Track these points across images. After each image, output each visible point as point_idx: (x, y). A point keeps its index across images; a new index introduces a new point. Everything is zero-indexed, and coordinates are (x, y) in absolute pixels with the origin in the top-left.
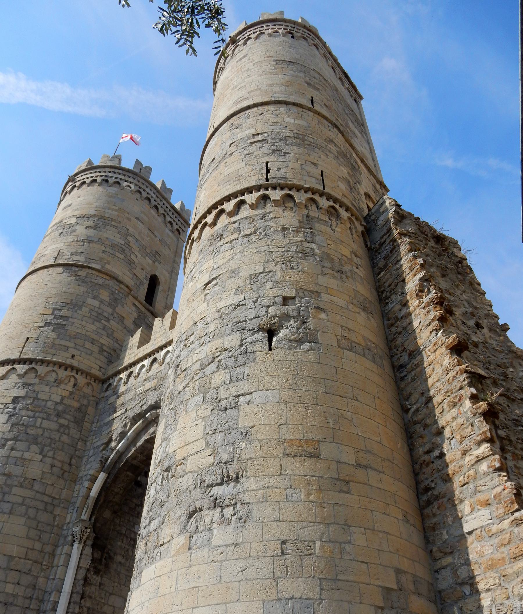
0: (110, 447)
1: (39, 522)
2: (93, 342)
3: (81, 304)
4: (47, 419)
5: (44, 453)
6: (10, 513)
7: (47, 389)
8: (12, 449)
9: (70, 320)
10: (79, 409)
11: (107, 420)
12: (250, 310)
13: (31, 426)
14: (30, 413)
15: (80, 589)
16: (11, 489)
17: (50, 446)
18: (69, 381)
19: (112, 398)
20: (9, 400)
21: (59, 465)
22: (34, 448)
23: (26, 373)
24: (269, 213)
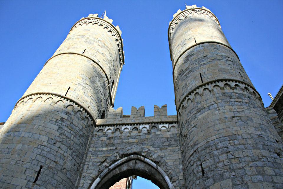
3: (94, 81)
4: (76, 137)
5: (73, 156)
7: (77, 120)
11: (101, 149)
12: (268, 142)
13: (69, 138)
18: (86, 120)
19: (103, 137)
21: (77, 165)
22: (69, 152)
24: (251, 97)
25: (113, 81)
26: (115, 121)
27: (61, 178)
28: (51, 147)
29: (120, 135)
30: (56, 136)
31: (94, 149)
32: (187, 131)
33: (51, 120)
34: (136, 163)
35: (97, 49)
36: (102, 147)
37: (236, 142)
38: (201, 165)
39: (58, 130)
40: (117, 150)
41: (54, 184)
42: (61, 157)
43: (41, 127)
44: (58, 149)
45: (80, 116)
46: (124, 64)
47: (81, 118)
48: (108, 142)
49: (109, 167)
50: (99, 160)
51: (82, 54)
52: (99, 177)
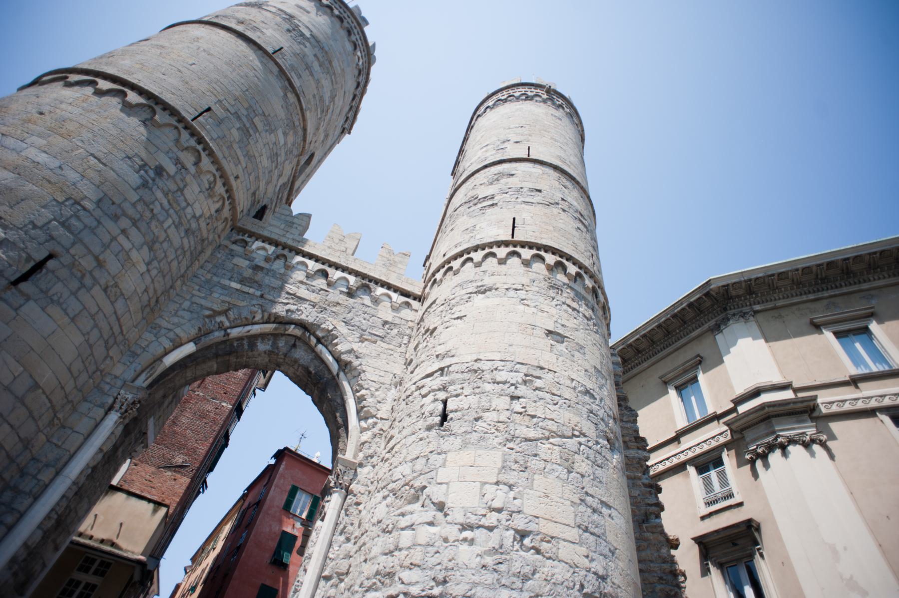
0: (218, 319)
1: (92, 354)
2: (257, 177)
4: (176, 227)
5: (150, 267)
6: (73, 319)
7: (197, 190)
8: (124, 231)
9: (257, 134)
10: (203, 240)
11: (226, 282)
14: (165, 202)
15: (83, 479)
16: (94, 285)
17: (159, 262)
18: (218, 202)
19: (242, 260)
20: (153, 164)
23: (186, 149)
25: (312, 155)
26: (284, 236)
27: (98, 305)
28: (102, 220)
29: (282, 271)
30: (126, 199)
31: (209, 276)
32: (439, 323)
33: (129, 158)
34: (294, 346)
35: (310, 64)
36: (230, 279)
37: (538, 383)
38: (445, 403)
39: (138, 188)
40: (263, 301)
41: (69, 311)
42: (121, 254)
43: (93, 161)
44: (119, 231)
45: (207, 186)
46: (349, 133)
47: (207, 190)
48: (248, 273)
49: (229, 331)
50: (209, 305)
51: (270, 50)
52: (196, 344)
